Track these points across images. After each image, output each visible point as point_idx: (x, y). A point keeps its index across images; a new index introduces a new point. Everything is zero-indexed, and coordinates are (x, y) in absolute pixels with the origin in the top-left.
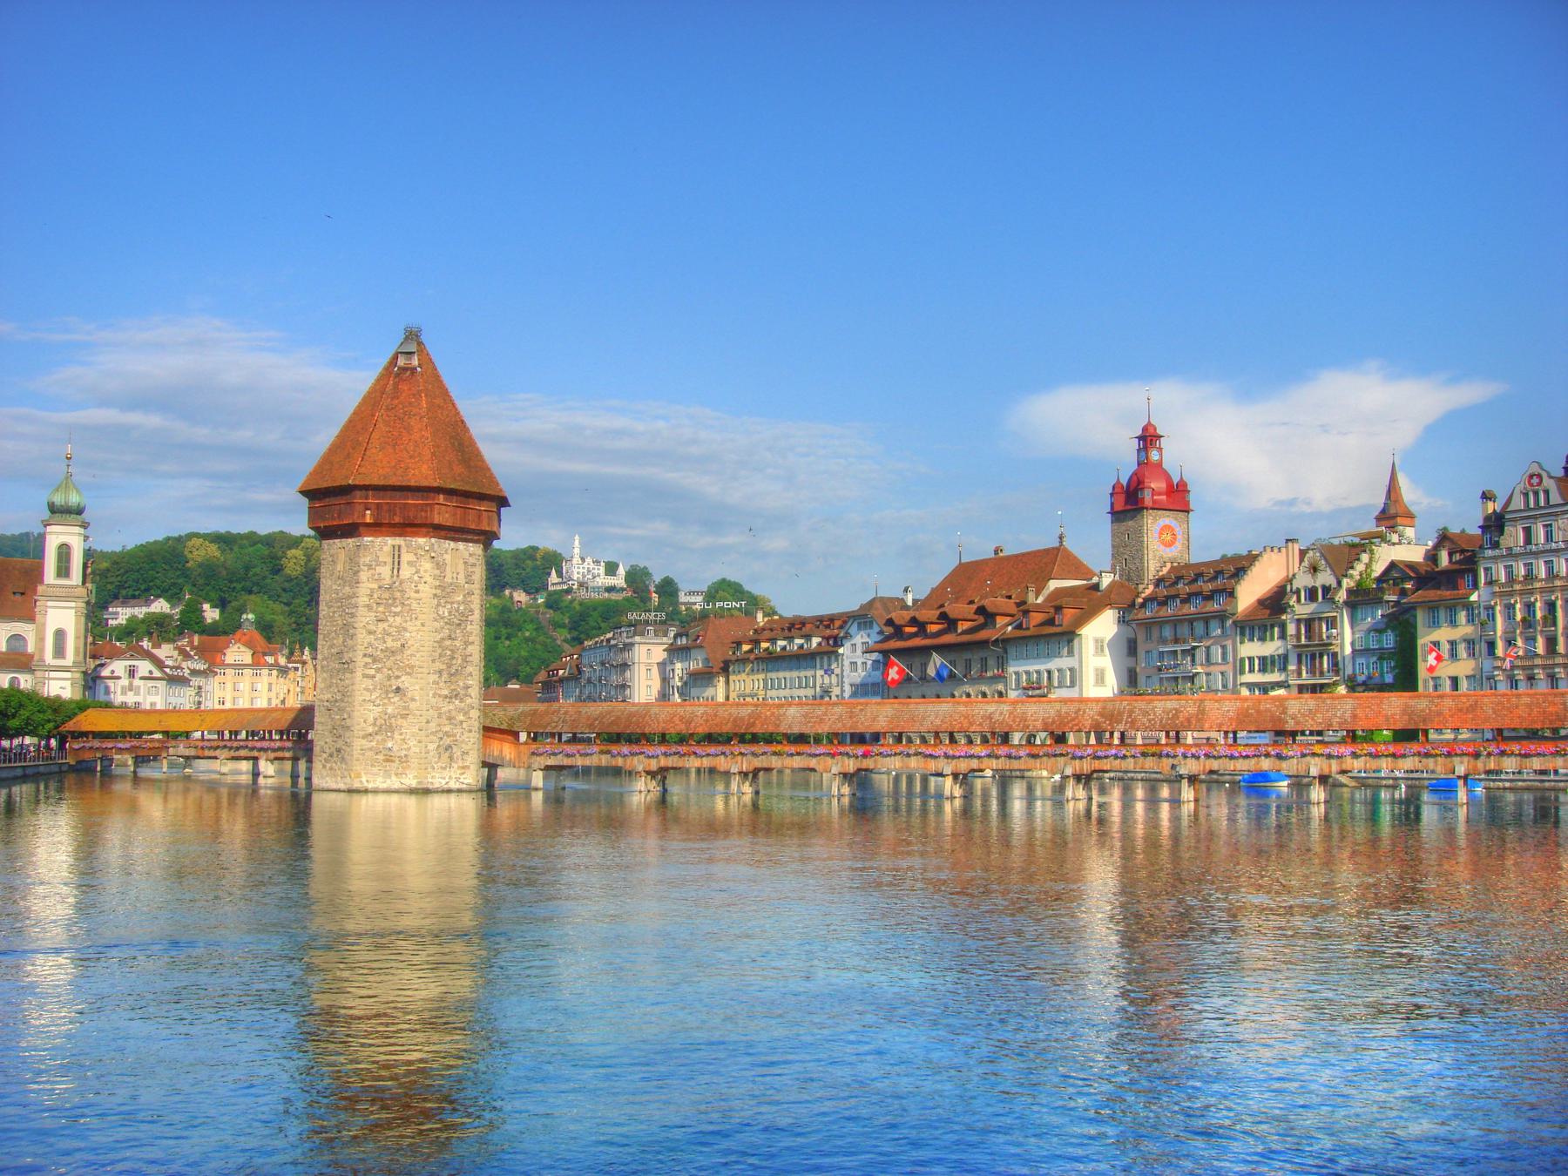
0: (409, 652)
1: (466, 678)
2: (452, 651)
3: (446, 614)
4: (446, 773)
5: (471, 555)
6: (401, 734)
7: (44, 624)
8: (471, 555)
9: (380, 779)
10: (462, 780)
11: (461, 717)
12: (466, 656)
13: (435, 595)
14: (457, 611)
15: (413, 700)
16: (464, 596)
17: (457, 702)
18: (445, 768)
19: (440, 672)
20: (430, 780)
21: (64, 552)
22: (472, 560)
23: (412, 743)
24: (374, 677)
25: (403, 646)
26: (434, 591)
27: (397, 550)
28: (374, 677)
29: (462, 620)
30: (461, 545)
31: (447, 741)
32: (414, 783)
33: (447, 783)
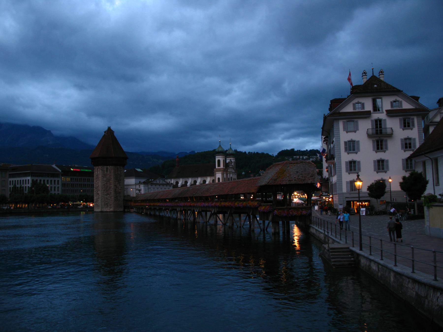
3: (105, 179)
4: (107, 208)
5: (111, 168)
7: (216, 177)
11: (109, 198)
13: (102, 176)
15: (100, 195)
17: (108, 196)
18: (106, 208)
19: (104, 190)
20: (103, 210)
21: (219, 161)
22: (111, 169)
25: (98, 186)
27: (98, 168)
30: (108, 167)
31: (106, 203)
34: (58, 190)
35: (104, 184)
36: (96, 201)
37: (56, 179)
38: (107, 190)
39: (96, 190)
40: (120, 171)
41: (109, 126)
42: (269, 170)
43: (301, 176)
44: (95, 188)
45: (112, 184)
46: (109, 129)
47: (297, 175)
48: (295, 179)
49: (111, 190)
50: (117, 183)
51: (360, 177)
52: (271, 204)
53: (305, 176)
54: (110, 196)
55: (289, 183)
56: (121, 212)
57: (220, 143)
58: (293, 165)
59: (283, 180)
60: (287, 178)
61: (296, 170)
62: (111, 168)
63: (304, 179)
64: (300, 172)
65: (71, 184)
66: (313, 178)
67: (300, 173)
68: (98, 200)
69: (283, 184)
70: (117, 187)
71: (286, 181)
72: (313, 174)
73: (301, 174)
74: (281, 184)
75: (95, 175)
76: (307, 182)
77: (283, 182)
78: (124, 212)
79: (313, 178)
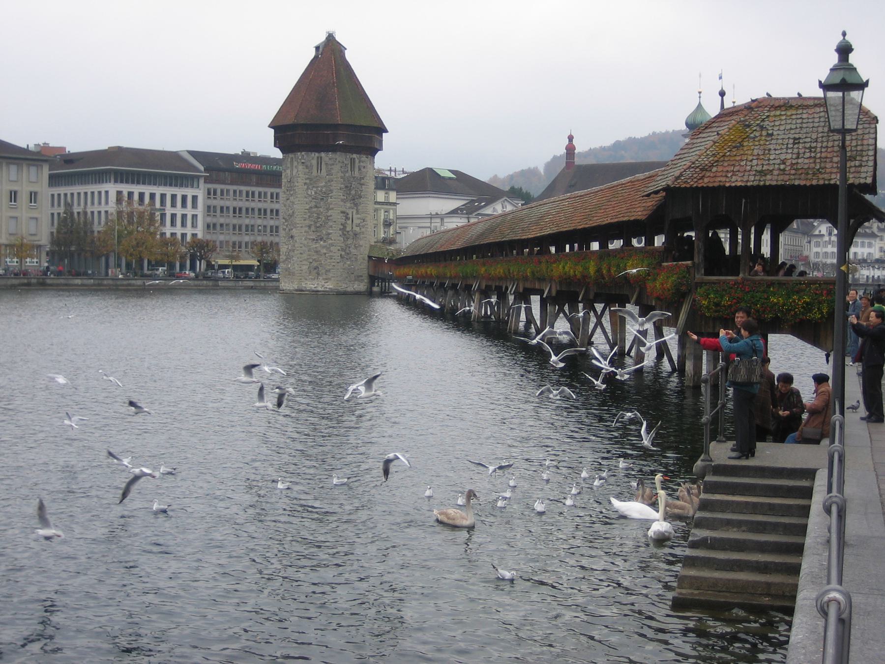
0: (295, 216)
1: (328, 229)
2: (318, 214)
3: (313, 193)
4: (316, 282)
6: (293, 260)
8: (330, 159)
9: (287, 285)
10: (326, 286)
11: (325, 251)
12: (328, 216)
13: (305, 184)
14: (321, 190)
15: (296, 242)
16: (326, 183)
17: (322, 243)
18: (314, 279)
19: (310, 227)
22: (331, 162)
23: (296, 265)
24: (285, 229)
26: (305, 181)
28: (285, 229)
29: (324, 196)
30: (323, 154)
32: (296, 288)
33: (315, 288)
34: (194, 225)
35: (311, 208)
36: (285, 258)
37: (190, 192)
38: (318, 225)
39: (286, 224)
40: (360, 169)
41: (331, 30)
42: (701, 135)
43: (807, 155)
44: (284, 218)
45: (332, 209)
46: (330, 38)
47: (796, 151)
48: (782, 167)
49: (331, 227)
50: (348, 205)
51: (853, 59)
52: (689, 262)
53: (823, 155)
54: (325, 244)
55: (756, 183)
56: (357, 293)
57: (700, 97)
58: (783, 113)
59: (736, 169)
60: (751, 161)
61: (792, 132)
62: (330, 159)
63: (818, 167)
64: (807, 140)
65: (235, 209)
66: (857, 163)
67: (808, 145)
68: (291, 254)
69: (733, 185)
70: (347, 218)
71: (747, 174)
72: (859, 148)
73: (811, 147)
74: (724, 186)
75: (284, 181)
76: (830, 180)
77: (734, 178)
78: (370, 294)
79: (855, 166)
